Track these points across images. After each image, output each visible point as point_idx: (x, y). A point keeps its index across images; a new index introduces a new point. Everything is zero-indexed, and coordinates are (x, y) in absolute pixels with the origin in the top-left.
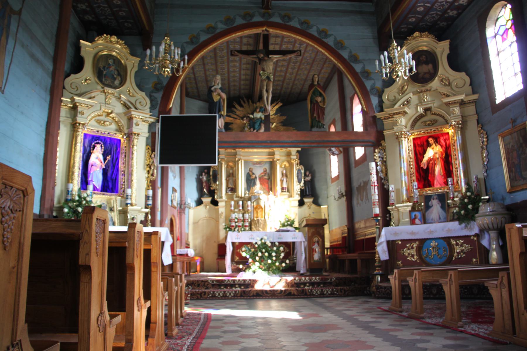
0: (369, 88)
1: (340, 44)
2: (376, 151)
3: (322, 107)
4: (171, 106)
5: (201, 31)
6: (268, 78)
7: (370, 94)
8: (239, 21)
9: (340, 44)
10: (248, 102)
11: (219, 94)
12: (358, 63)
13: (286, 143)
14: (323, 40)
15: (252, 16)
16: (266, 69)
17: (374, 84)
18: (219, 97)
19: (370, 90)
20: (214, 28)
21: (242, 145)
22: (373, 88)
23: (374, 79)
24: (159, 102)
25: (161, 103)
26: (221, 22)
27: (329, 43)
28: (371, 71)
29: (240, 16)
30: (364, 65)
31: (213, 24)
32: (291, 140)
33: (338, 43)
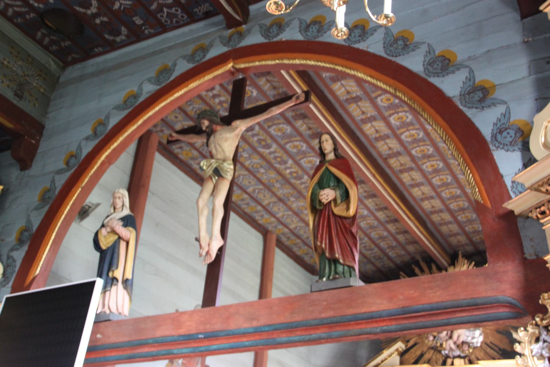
0: (486, 131)
1: (400, 42)
2: (520, 335)
3: (341, 217)
4: (38, 272)
5: (113, 109)
6: (217, 172)
7: (491, 147)
8: (183, 67)
9: (400, 42)
10: (430, 269)
11: (113, 232)
12: (453, 72)
13: (245, 334)
14: (356, 46)
15: (204, 50)
16: (214, 152)
17: (507, 114)
18: (114, 238)
19: (494, 137)
20: (135, 96)
21: (145, 350)
22: (500, 130)
23: (505, 103)
24: (17, 269)
25: (19, 270)
26: (149, 80)
27: (371, 50)
28: (496, 83)
29: (184, 57)
30: (471, 71)
31: (135, 89)
32: (255, 324)
33: (396, 40)
